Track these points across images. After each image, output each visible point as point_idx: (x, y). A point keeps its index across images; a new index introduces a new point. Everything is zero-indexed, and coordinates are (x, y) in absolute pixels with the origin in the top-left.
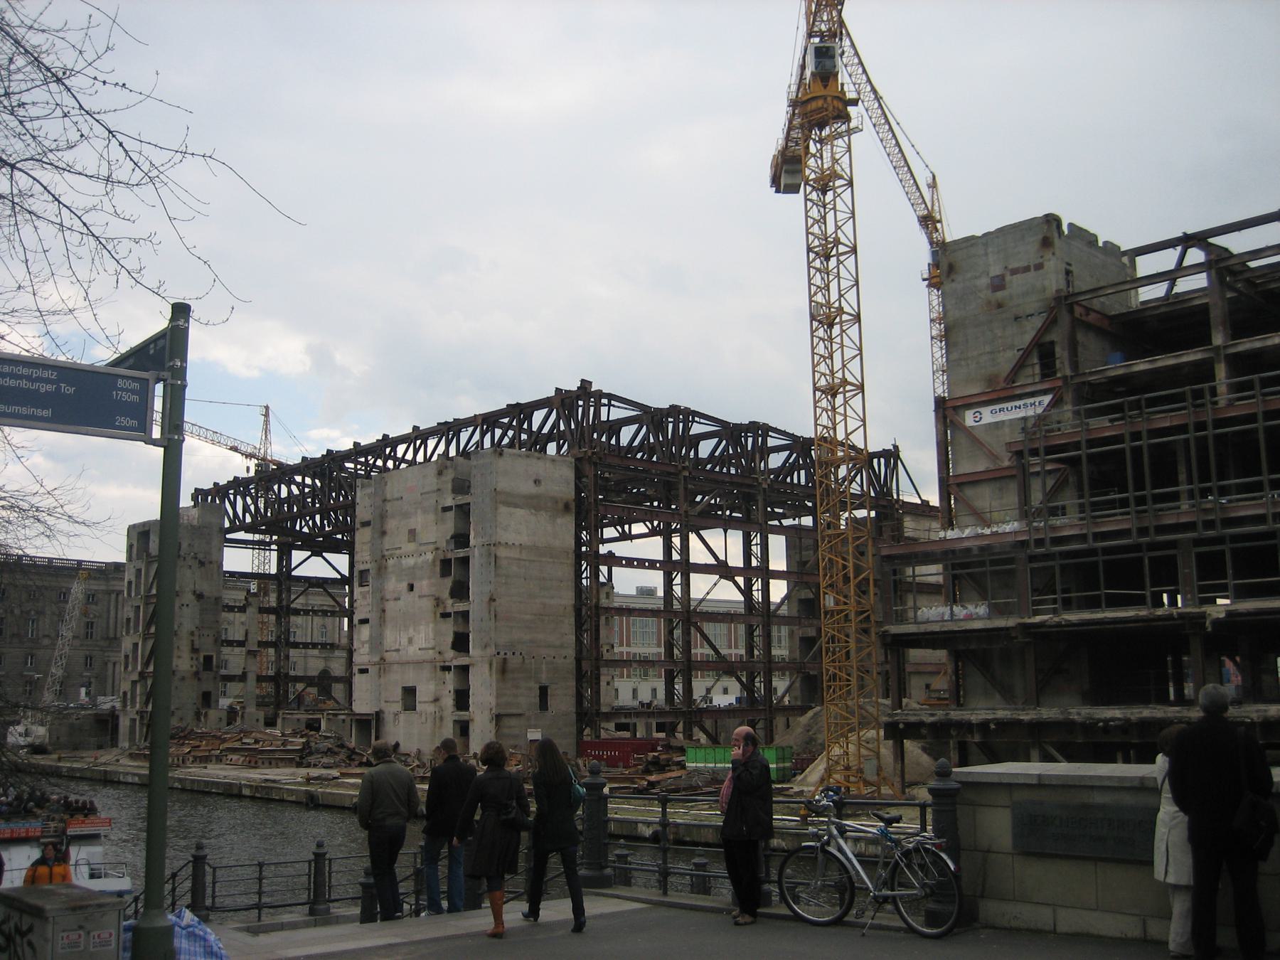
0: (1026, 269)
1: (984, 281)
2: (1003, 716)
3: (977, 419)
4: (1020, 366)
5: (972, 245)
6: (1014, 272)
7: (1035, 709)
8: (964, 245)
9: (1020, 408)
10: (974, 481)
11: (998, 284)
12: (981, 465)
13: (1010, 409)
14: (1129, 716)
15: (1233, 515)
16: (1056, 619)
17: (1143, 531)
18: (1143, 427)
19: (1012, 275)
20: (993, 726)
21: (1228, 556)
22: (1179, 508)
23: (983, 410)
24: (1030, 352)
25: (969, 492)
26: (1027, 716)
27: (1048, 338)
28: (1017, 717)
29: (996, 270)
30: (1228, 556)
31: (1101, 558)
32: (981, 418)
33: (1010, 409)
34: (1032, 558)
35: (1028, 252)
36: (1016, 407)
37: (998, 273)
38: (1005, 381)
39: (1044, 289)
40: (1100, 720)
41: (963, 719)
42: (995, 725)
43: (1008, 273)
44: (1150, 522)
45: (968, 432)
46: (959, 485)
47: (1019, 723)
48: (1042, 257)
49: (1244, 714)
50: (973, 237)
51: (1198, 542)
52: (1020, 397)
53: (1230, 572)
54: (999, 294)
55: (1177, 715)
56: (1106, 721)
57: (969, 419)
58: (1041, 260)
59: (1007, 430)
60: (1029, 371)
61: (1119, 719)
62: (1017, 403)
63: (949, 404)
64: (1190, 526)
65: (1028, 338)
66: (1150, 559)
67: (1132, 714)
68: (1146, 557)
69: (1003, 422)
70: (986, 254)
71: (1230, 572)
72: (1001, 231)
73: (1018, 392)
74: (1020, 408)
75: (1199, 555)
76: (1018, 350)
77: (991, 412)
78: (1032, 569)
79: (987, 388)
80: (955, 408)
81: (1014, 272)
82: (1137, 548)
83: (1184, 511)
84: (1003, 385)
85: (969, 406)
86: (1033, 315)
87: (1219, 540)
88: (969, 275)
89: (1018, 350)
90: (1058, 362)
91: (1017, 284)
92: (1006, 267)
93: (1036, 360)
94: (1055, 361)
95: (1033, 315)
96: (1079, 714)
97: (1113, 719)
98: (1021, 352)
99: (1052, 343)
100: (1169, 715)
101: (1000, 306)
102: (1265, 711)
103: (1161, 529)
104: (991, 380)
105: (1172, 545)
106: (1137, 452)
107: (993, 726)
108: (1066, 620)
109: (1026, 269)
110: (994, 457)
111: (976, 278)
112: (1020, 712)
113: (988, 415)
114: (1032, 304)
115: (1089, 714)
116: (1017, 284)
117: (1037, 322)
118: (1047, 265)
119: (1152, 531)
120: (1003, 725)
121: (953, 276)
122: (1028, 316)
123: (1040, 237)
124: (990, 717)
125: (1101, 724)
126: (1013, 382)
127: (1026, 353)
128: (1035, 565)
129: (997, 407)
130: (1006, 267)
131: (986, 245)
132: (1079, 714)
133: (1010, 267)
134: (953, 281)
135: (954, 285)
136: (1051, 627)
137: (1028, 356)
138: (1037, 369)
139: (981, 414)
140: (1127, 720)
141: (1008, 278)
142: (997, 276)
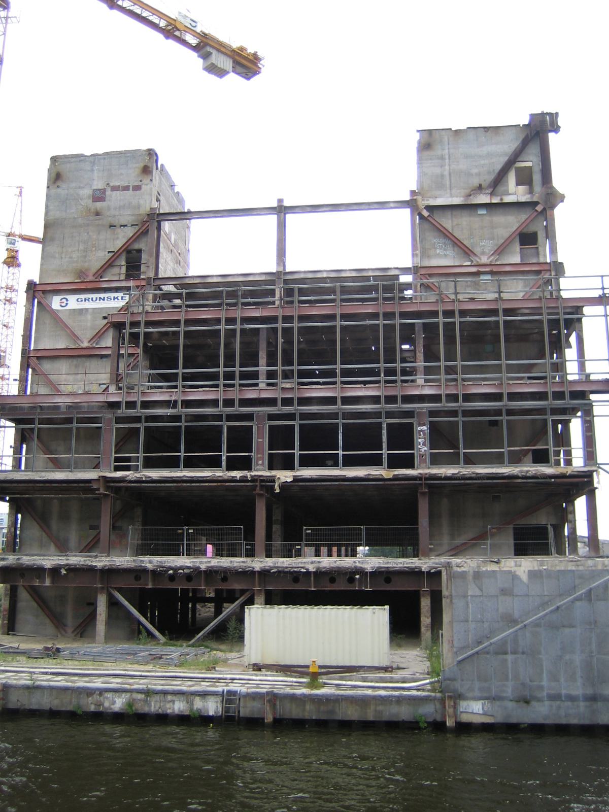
0: (126, 188)
1: (86, 192)
2: (75, 562)
3: (63, 305)
4: (109, 264)
5: (81, 161)
6: (115, 188)
7: (107, 557)
8: (73, 160)
9: (104, 300)
10: (54, 356)
11: (99, 196)
12: (61, 344)
13: (94, 299)
14: (198, 565)
15: (307, 395)
16: (138, 475)
17: (229, 403)
18: (238, 313)
19: (112, 190)
20: (63, 572)
22: (257, 385)
23: (70, 297)
24: (120, 255)
25: (46, 366)
26: (101, 562)
27: (136, 246)
28: (90, 563)
29: (99, 185)
31: (183, 424)
32: (67, 304)
33: (94, 299)
34: (119, 420)
35: (130, 175)
36: (100, 298)
37: (100, 187)
38: (94, 276)
39: (139, 207)
40: (170, 568)
41: (34, 564)
42: (66, 570)
43: (109, 189)
44: (235, 394)
45: (54, 314)
46: (38, 358)
47: (91, 570)
48: (141, 181)
49: (300, 565)
50: (82, 155)
51: (272, 417)
52: (106, 290)
53: (297, 444)
54: (99, 205)
55: (242, 564)
56: (176, 569)
57: (56, 303)
58: (140, 183)
59: (89, 317)
60: (116, 270)
61: (188, 568)
62: (102, 295)
63: (39, 288)
64: (272, 402)
65: (119, 243)
66: (228, 427)
67: (201, 563)
68: (225, 425)
69: (87, 309)
70: (92, 170)
71: (297, 444)
72: (108, 154)
73: (105, 285)
74: (104, 300)
76: (109, 252)
77: (77, 300)
79: (77, 279)
80: (44, 292)
81: (115, 188)
82: (218, 418)
83: (261, 390)
84: (91, 278)
85: (57, 292)
86: (126, 226)
88: (74, 185)
89: (109, 252)
90: (142, 266)
91: (114, 198)
92: (108, 184)
93: (123, 263)
94: (140, 265)
95: (126, 226)
96: (150, 562)
97: (182, 568)
98: (111, 254)
99: (139, 251)
100: (235, 565)
101: (97, 214)
102: (319, 562)
103: (245, 402)
104: (81, 273)
105: (249, 417)
106: (231, 334)
107: (63, 572)
108: (146, 477)
109: (126, 188)
110: (74, 337)
111: (80, 188)
112: (93, 559)
113: (74, 302)
114: (127, 217)
115: (161, 562)
116: (114, 198)
117: (130, 232)
118: (144, 187)
119: (237, 403)
120: (73, 570)
121: (59, 183)
122: (121, 226)
123: (142, 165)
125: (171, 572)
126: (101, 278)
127: (116, 255)
128: (122, 426)
129: (83, 296)
130: (108, 184)
131: (93, 163)
132: (150, 562)
133: (112, 184)
134: (58, 187)
135: (59, 190)
136: (131, 482)
137: (118, 257)
138: (124, 270)
139: (67, 300)
140: (197, 570)
141: (108, 192)
142: (99, 190)
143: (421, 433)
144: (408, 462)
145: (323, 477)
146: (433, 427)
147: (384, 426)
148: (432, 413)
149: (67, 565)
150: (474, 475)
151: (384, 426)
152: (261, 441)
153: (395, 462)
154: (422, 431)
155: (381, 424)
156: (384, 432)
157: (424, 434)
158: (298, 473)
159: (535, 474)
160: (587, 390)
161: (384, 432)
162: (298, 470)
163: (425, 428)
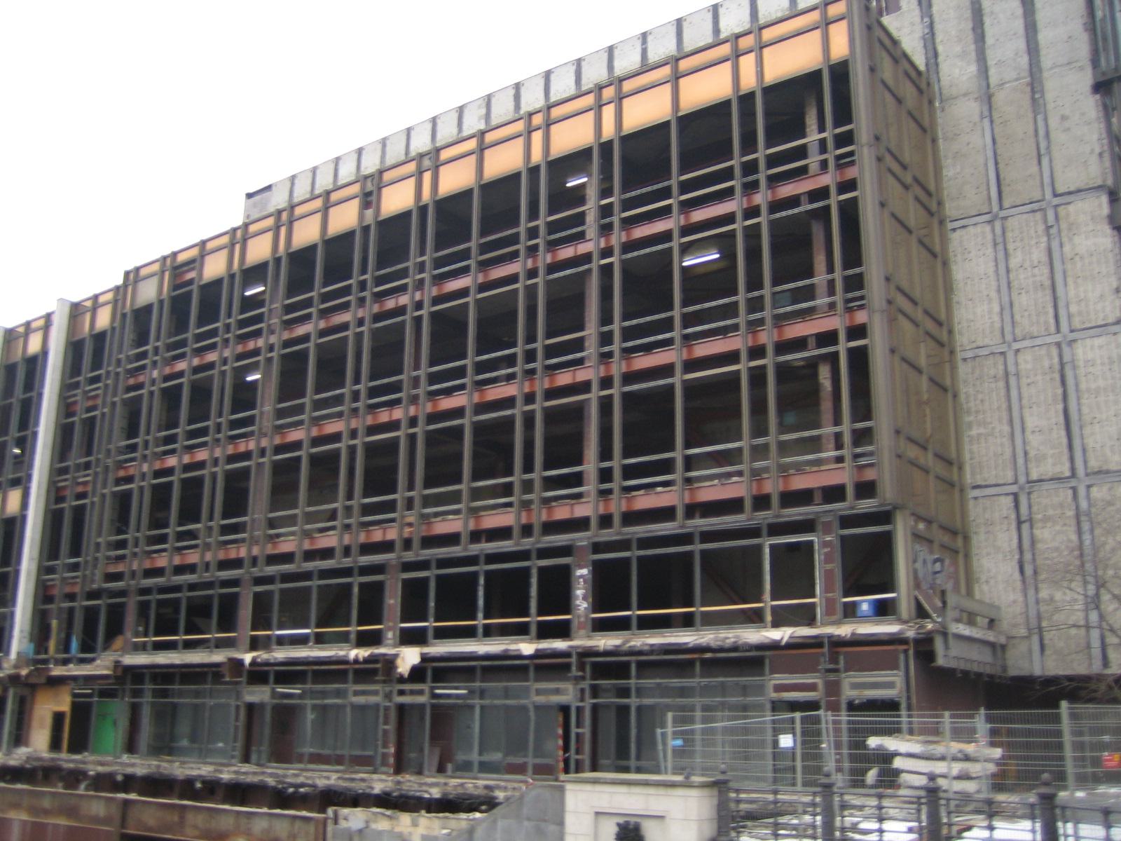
20: (199, 785)
21: (432, 585)
30: (432, 585)
40: (292, 785)
66: (362, 585)
75: (405, 582)
78: (256, 595)
87: (424, 565)
108: (276, 658)
124: (195, 773)
125: (291, 790)
143: (581, 580)
144: (563, 631)
145: (457, 655)
146: (598, 567)
147: (534, 572)
148: (597, 548)
149: (200, 776)
150: (646, 648)
151: (534, 572)
152: (393, 601)
153: (546, 631)
154: (581, 576)
155: (527, 570)
156: (534, 581)
157: (585, 582)
158: (426, 650)
159: (735, 642)
160: (816, 486)
161: (534, 581)
162: (433, 645)
163: (584, 571)
